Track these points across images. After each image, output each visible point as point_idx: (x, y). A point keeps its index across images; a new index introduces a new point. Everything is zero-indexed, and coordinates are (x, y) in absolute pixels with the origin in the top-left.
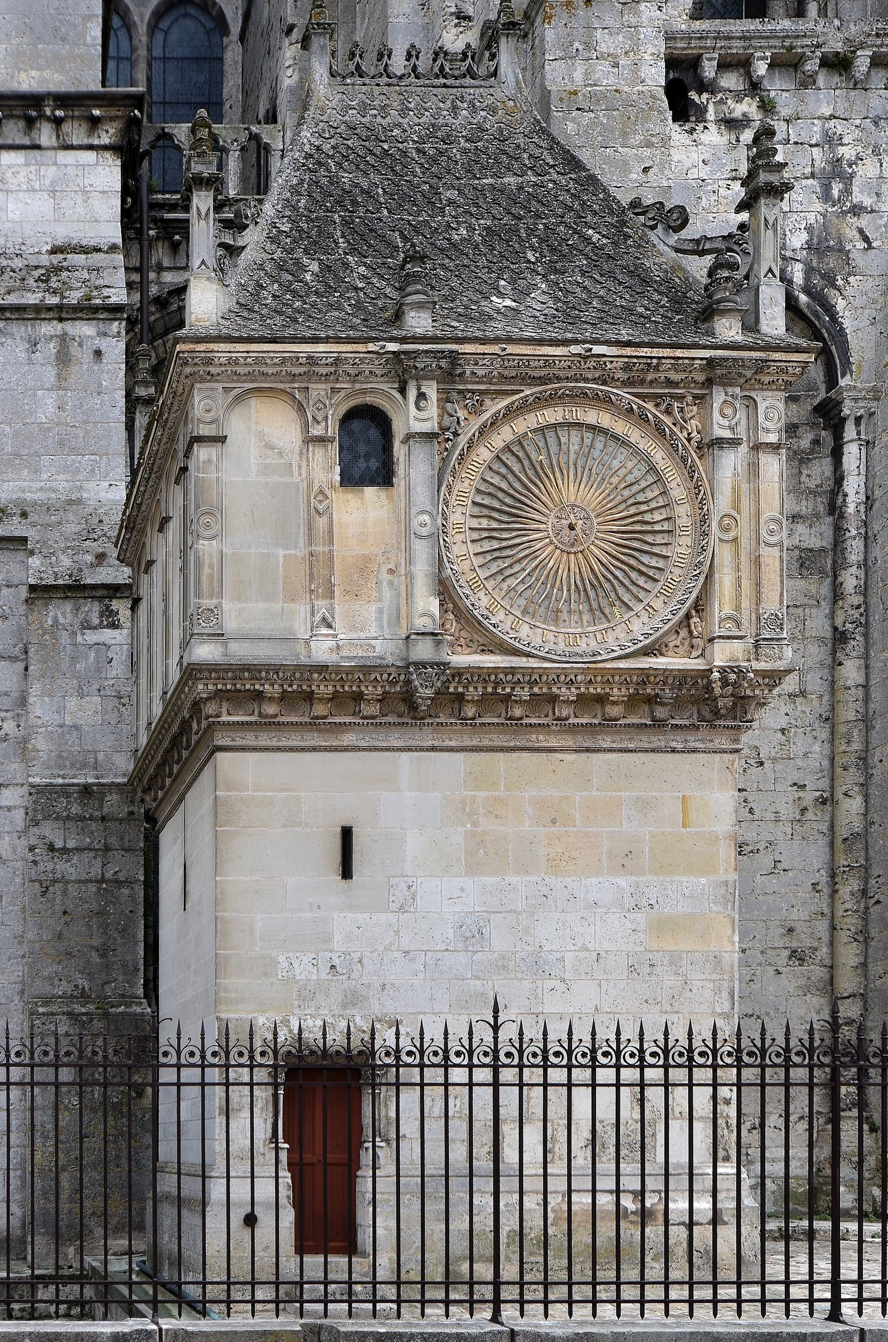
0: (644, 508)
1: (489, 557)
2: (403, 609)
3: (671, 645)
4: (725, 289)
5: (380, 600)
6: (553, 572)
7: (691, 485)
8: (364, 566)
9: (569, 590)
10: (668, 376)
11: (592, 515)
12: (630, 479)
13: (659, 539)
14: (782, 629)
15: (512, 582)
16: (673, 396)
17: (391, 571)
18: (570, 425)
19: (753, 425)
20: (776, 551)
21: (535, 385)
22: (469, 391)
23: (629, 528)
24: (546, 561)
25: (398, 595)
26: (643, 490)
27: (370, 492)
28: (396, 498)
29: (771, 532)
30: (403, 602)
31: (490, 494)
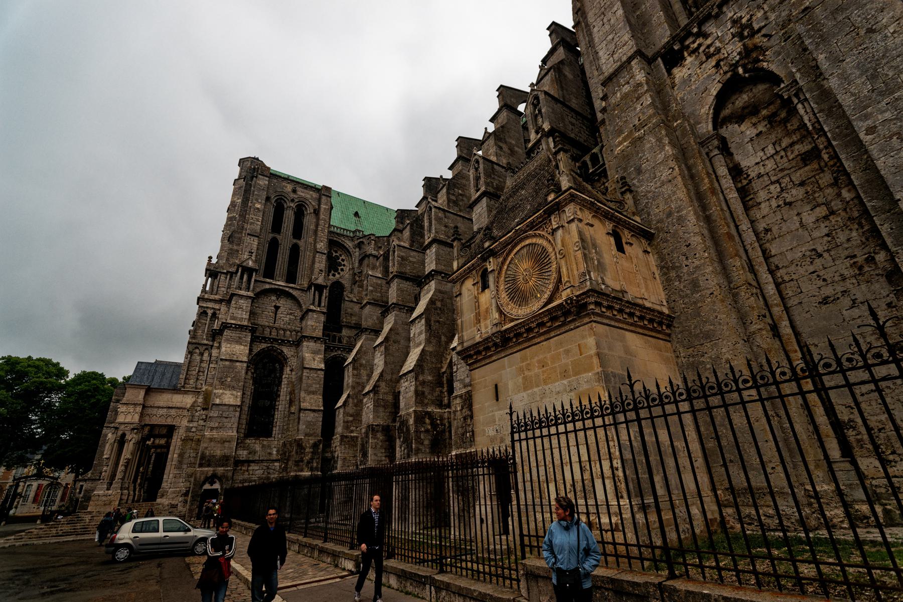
8: (487, 311)
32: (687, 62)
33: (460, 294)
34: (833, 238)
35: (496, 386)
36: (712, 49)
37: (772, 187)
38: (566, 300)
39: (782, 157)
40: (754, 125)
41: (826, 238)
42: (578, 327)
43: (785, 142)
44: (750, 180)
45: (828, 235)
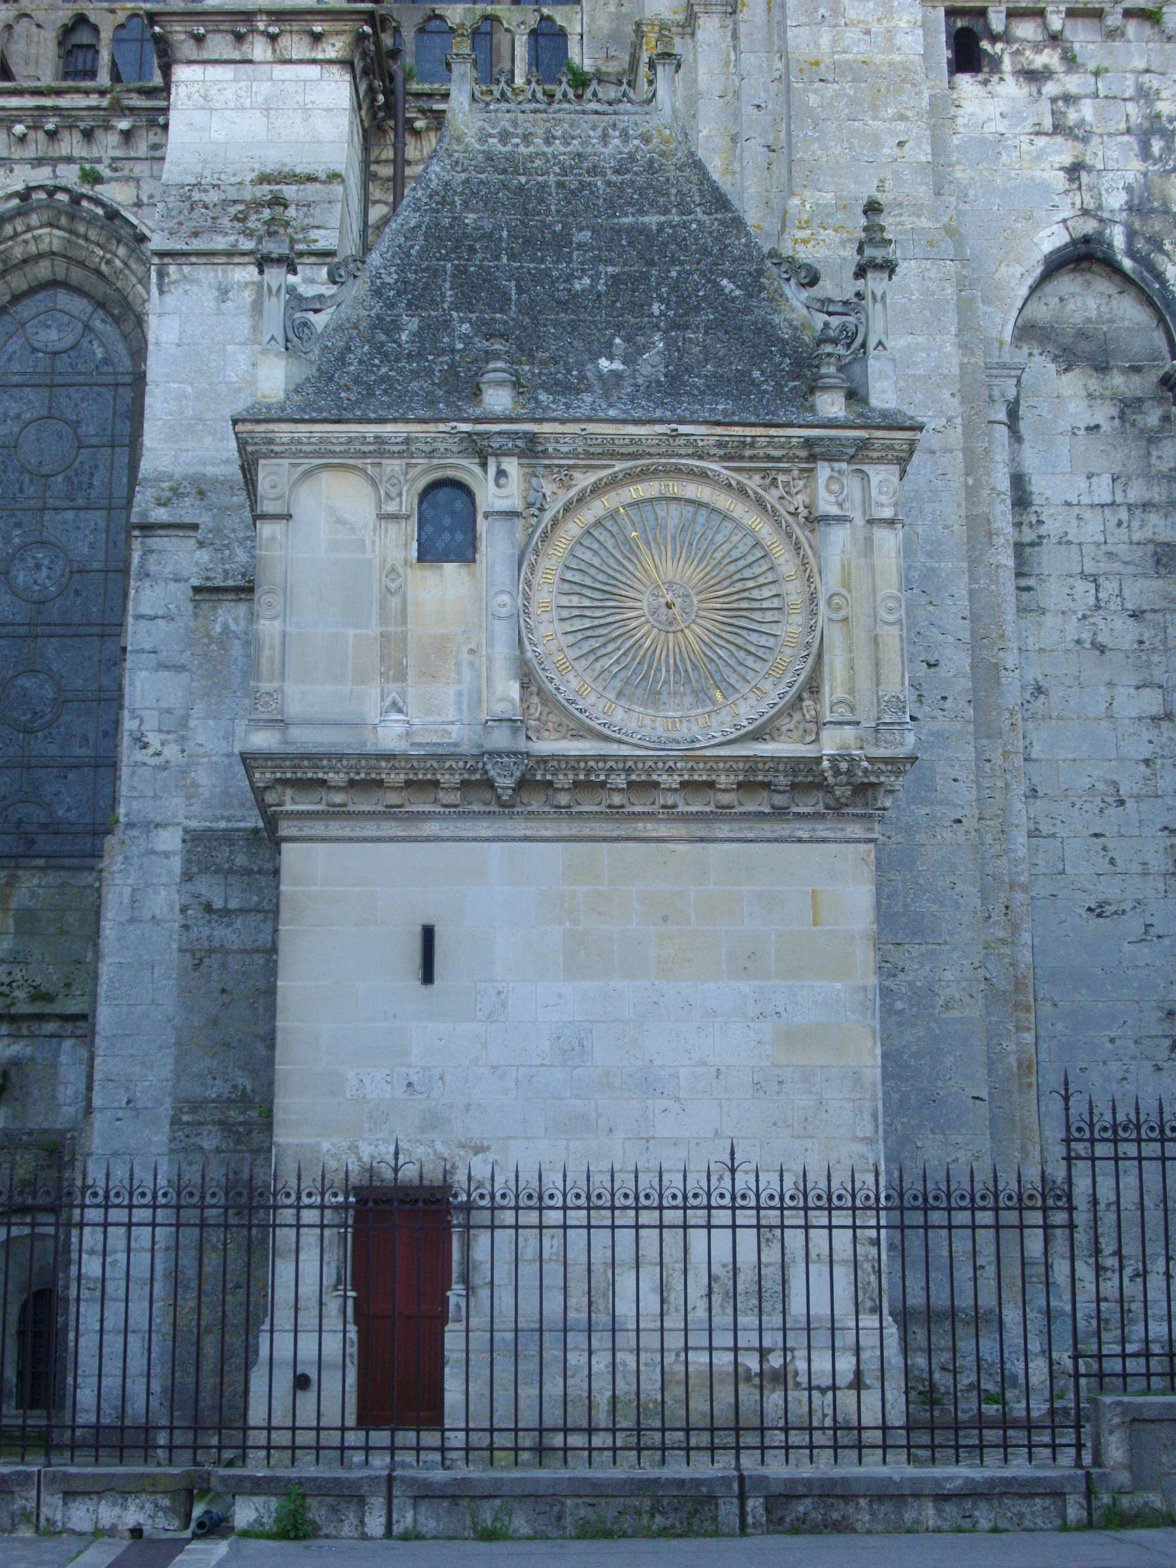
0: (751, 584)
1: (580, 636)
2: (484, 691)
3: (784, 728)
4: (829, 364)
5: (460, 682)
8: (442, 646)
9: (668, 671)
11: (692, 593)
12: (736, 554)
13: (769, 616)
15: (606, 662)
16: (779, 470)
17: (472, 652)
18: (668, 499)
19: (866, 500)
20: (895, 630)
23: (734, 605)
25: (480, 676)
26: (749, 565)
27: (450, 568)
29: (890, 610)
30: (484, 684)
32: (1000, 89)
33: (289, 517)
34: (1154, 774)
35: (428, 934)
36: (1072, 116)
37: (1082, 586)
38: (833, 759)
39: (1120, 524)
40: (1090, 396)
41: (1142, 767)
42: (824, 840)
43: (1137, 492)
44: (1040, 537)
45: (1147, 762)
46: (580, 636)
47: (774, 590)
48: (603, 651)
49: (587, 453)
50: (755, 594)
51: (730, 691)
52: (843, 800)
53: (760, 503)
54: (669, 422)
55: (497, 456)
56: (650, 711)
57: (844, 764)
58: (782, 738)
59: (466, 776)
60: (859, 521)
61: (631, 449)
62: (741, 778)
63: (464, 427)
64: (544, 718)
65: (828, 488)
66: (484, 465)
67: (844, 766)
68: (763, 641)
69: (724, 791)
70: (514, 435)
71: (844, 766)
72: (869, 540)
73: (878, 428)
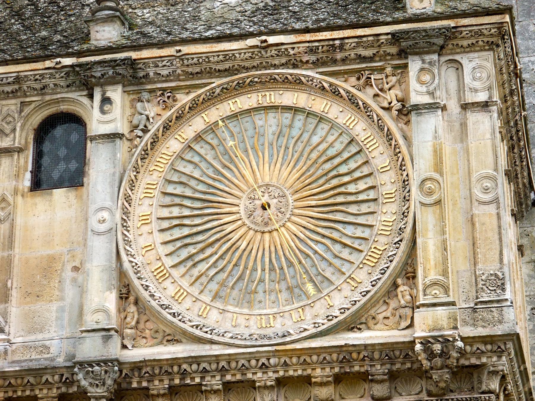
0: (346, 179)
1: (179, 244)
5: (62, 299)
6: (246, 253)
7: (392, 153)
8: (49, 267)
9: (263, 270)
10: (359, 53)
11: (287, 193)
12: (331, 152)
13: (364, 208)
14: (503, 290)
16: (373, 70)
17: (76, 269)
21: (226, 77)
22: (160, 89)
24: (239, 243)
26: (345, 161)
27: (58, 193)
28: (85, 197)
29: (486, 190)
31: (181, 183)
38: (426, 342)
46: (179, 244)
47: (370, 182)
48: (201, 256)
49: (186, 73)
50: (351, 188)
51: (326, 283)
52: (442, 385)
53: (352, 101)
54: (260, 34)
55: (102, 86)
56: (246, 311)
57: (439, 347)
58: (379, 326)
59: (64, 390)
60: (454, 106)
61: (227, 65)
62: (337, 370)
63: (68, 61)
64: (141, 326)
65: (418, 81)
66: (91, 96)
67: (437, 348)
68: (359, 232)
69: (322, 384)
70: (114, 63)
71: (437, 348)
72: (464, 125)
73: (464, 15)
